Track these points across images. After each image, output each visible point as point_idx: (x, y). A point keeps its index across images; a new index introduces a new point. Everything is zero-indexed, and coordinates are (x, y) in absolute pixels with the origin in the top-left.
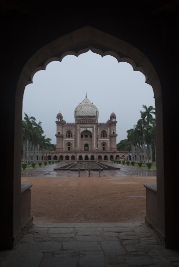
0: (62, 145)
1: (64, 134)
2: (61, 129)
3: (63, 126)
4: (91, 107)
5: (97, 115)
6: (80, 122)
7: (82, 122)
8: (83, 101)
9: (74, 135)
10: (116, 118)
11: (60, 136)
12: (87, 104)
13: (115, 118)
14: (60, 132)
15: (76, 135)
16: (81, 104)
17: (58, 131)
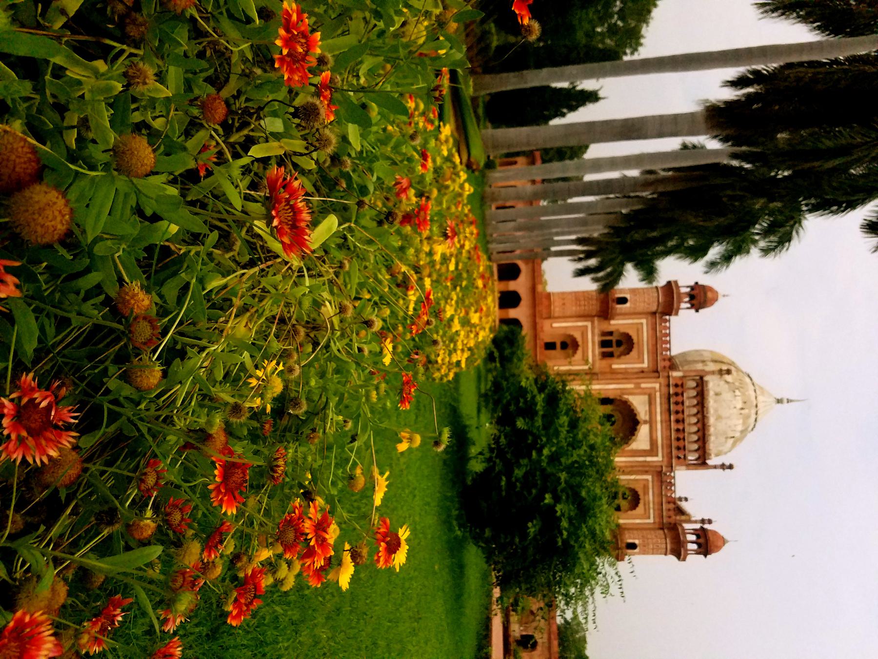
0: (565, 318)
1: (618, 324)
2: (641, 307)
3: (654, 313)
4: (740, 428)
5: (715, 467)
6: (676, 394)
7: (677, 403)
8: (761, 388)
9: (614, 366)
10: (702, 556)
11: (608, 307)
12: (753, 411)
13: (698, 553)
14: (628, 305)
15: (614, 375)
16: (748, 380)
17: (628, 296)
